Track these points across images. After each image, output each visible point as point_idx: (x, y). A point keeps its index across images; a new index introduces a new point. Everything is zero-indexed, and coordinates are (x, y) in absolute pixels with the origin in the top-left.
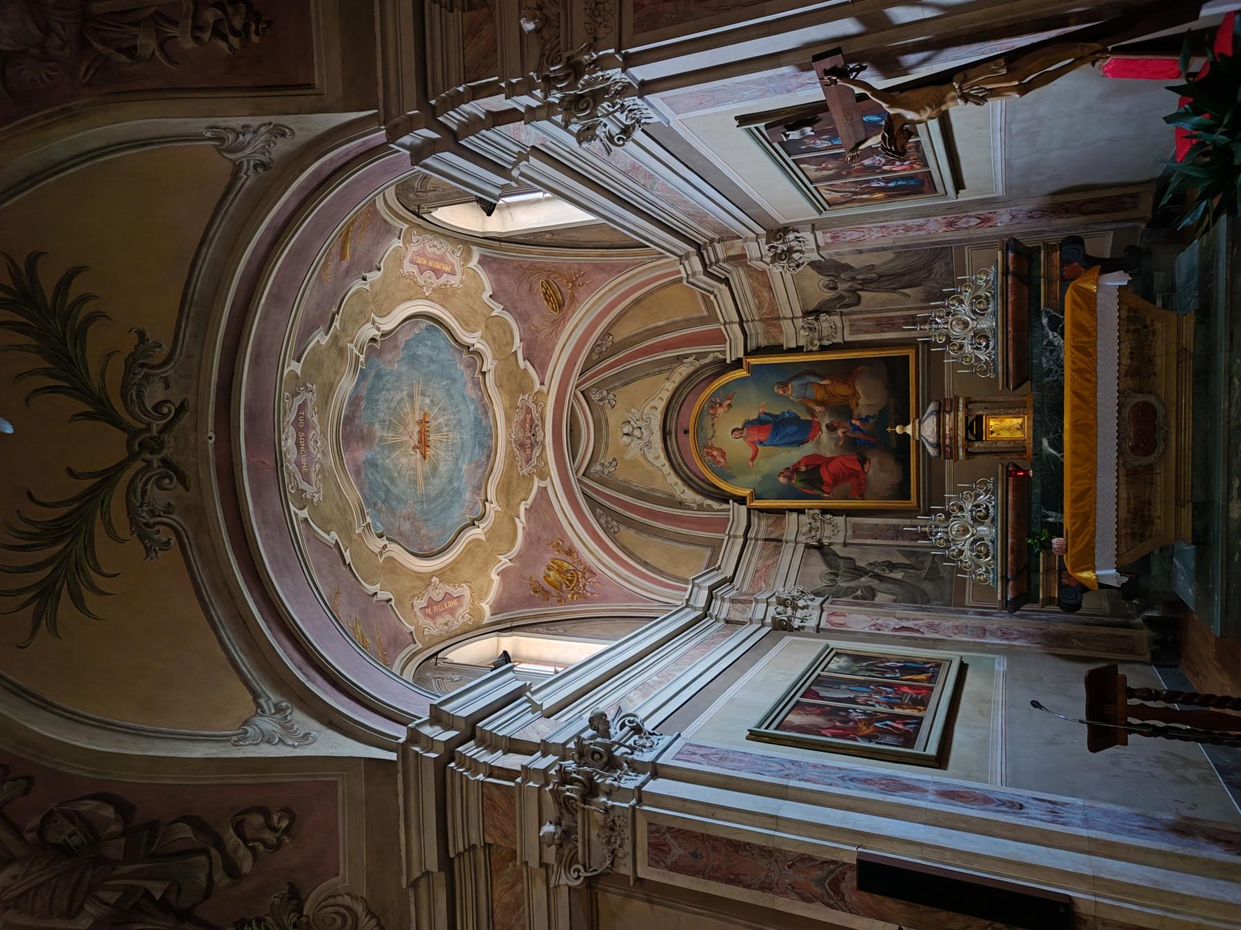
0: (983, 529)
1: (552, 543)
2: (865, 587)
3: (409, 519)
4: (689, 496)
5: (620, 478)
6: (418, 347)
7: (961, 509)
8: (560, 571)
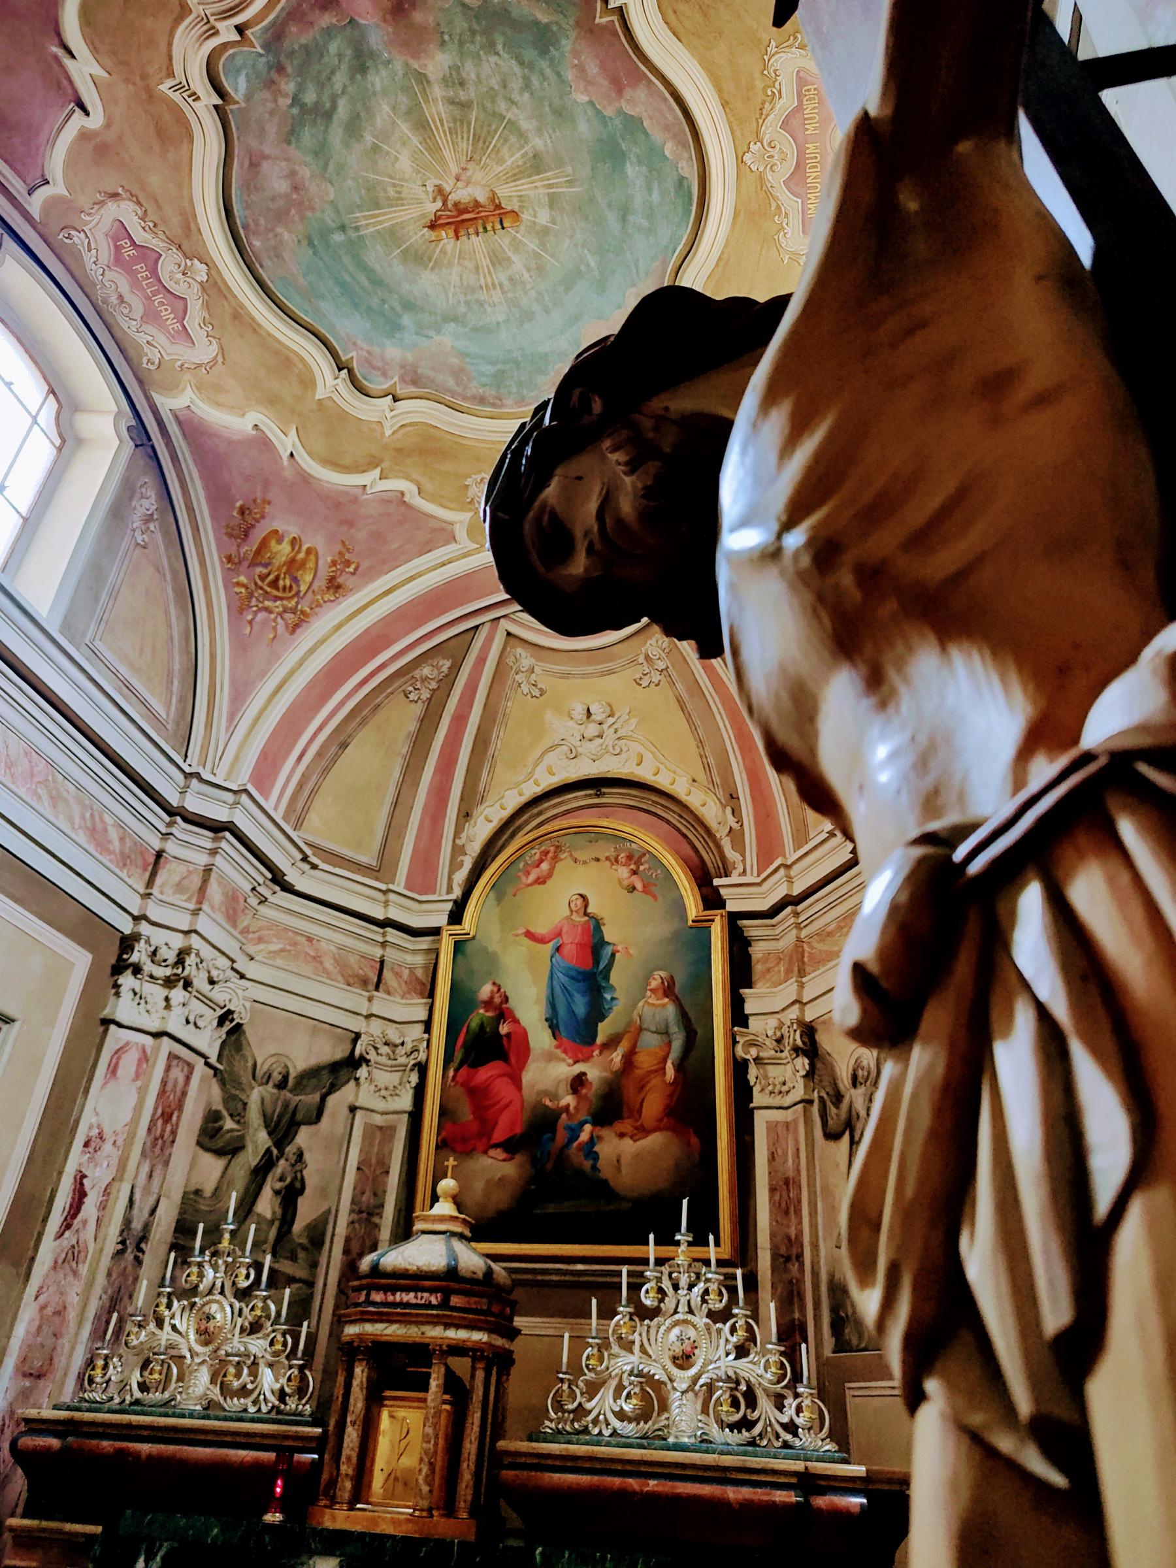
0: (201, 1383)
1: (348, 550)
2: (242, 1138)
3: (296, 188)
4: (481, 830)
5: (509, 704)
6: (640, 163)
7: (254, 1328)
8: (293, 565)
